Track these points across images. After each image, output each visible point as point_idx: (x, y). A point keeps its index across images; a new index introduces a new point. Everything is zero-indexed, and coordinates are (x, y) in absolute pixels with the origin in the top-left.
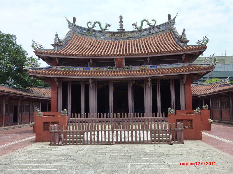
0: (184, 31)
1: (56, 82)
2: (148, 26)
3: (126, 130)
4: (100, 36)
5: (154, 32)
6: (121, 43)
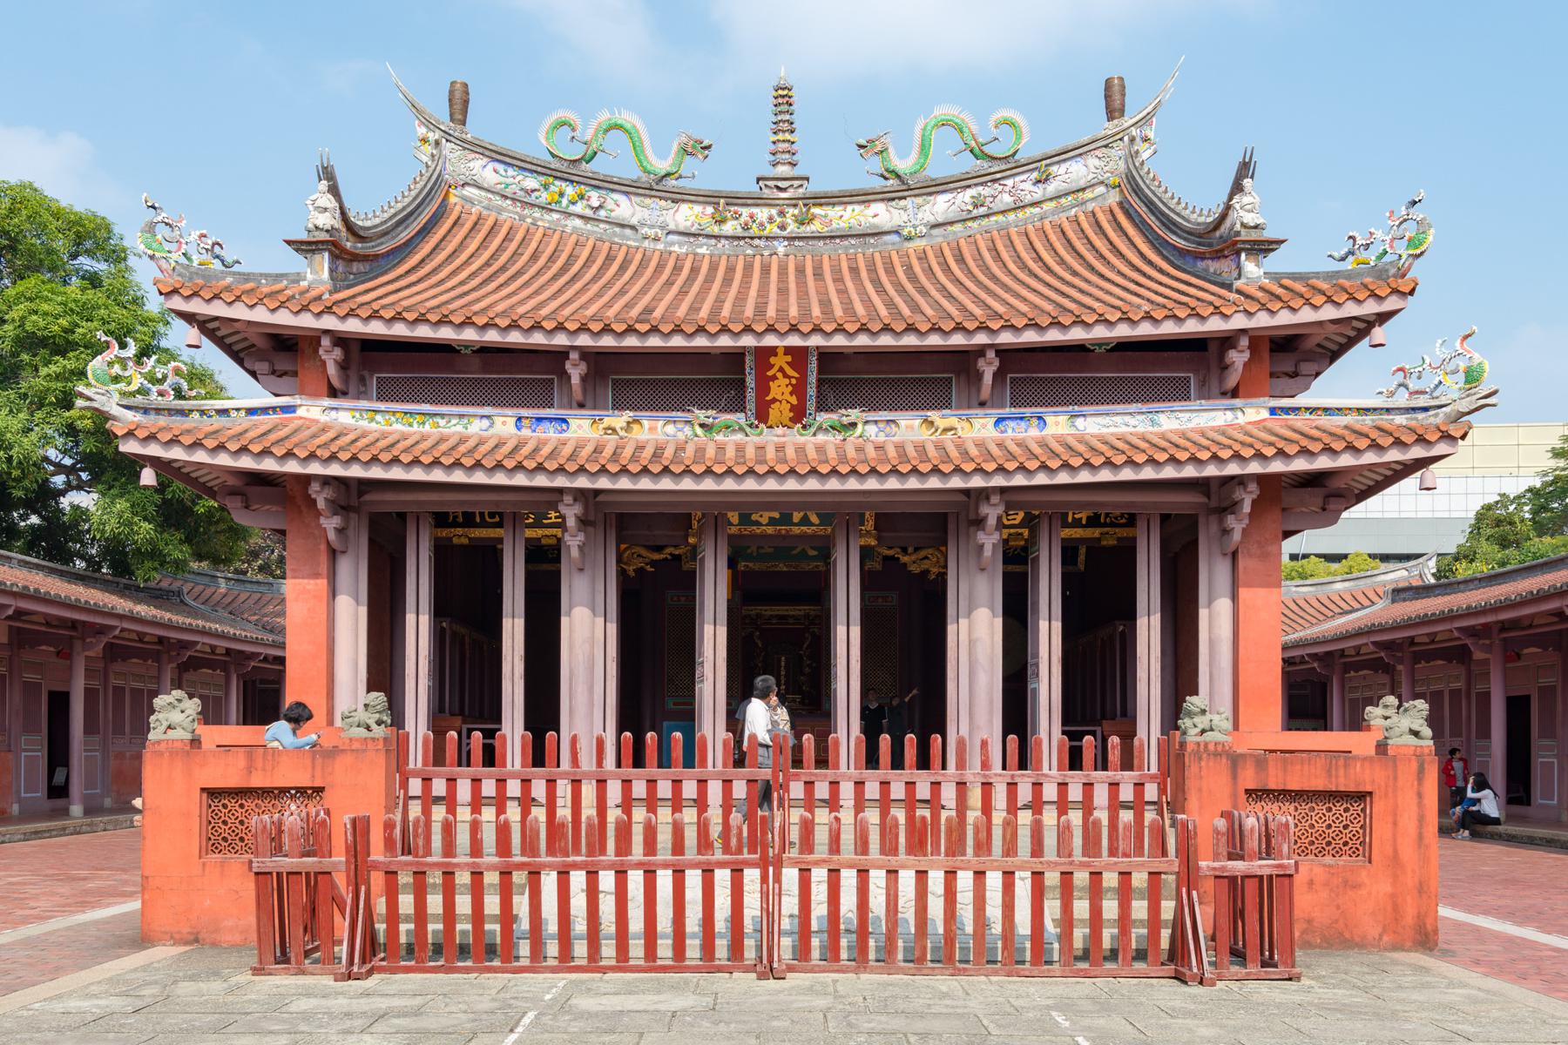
2: (969, 164)
4: (634, 221)
5: (1007, 199)
6: (783, 271)
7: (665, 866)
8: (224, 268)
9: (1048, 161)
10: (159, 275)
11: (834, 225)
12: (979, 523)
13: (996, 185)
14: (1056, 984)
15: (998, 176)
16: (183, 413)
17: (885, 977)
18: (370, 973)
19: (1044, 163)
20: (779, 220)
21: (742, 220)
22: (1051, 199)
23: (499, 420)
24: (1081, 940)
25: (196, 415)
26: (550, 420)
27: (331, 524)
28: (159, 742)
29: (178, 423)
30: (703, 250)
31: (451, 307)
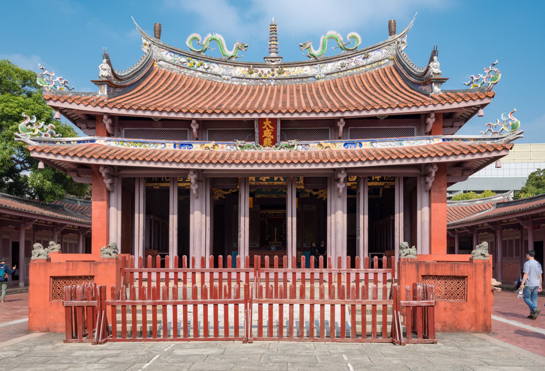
4: (220, 73)
5: (353, 64)
7: (170, 303)
9: (368, 51)
11: (291, 74)
12: (338, 180)
13: (349, 60)
14: (349, 345)
15: (350, 56)
16: (54, 142)
17: (288, 342)
18: (105, 342)
19: (366, 51)
20: (272, 72)
21: (259, 73)
22: (369, 64)
23: (167, 145)
24: (130, 328)
25: (59, 143)
26: (186, 145)
27: (107, 182)
28: (35, 260)
29: (52, 146)
30: (245, 84)
31: (150, 104)
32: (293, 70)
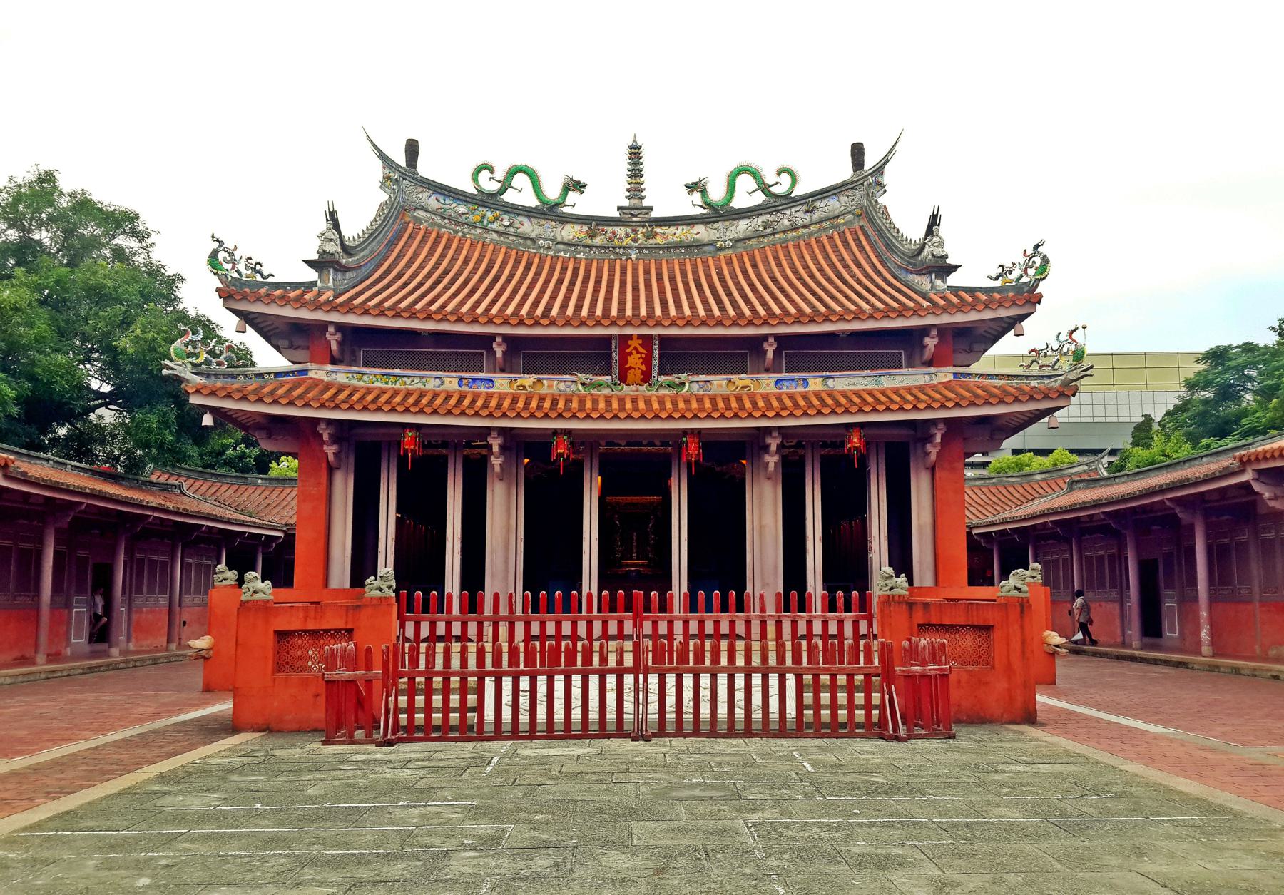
0: (934, 220)
1: (323, 443)
2: (759, 198)
3: (688, 672)
4: (533, 235)
5: (786, 222)
6: (635, 270)
8: (262, 280)
10: (221, 286)
11: (670, 240)
13: (779, 214)
15: (780, 208)
16: (233, 376)
20: (633, 235)
21: (608, 235)
22: (816, 223)
26: (482, 380)
30: (581, 256)
32: (674, 232)
